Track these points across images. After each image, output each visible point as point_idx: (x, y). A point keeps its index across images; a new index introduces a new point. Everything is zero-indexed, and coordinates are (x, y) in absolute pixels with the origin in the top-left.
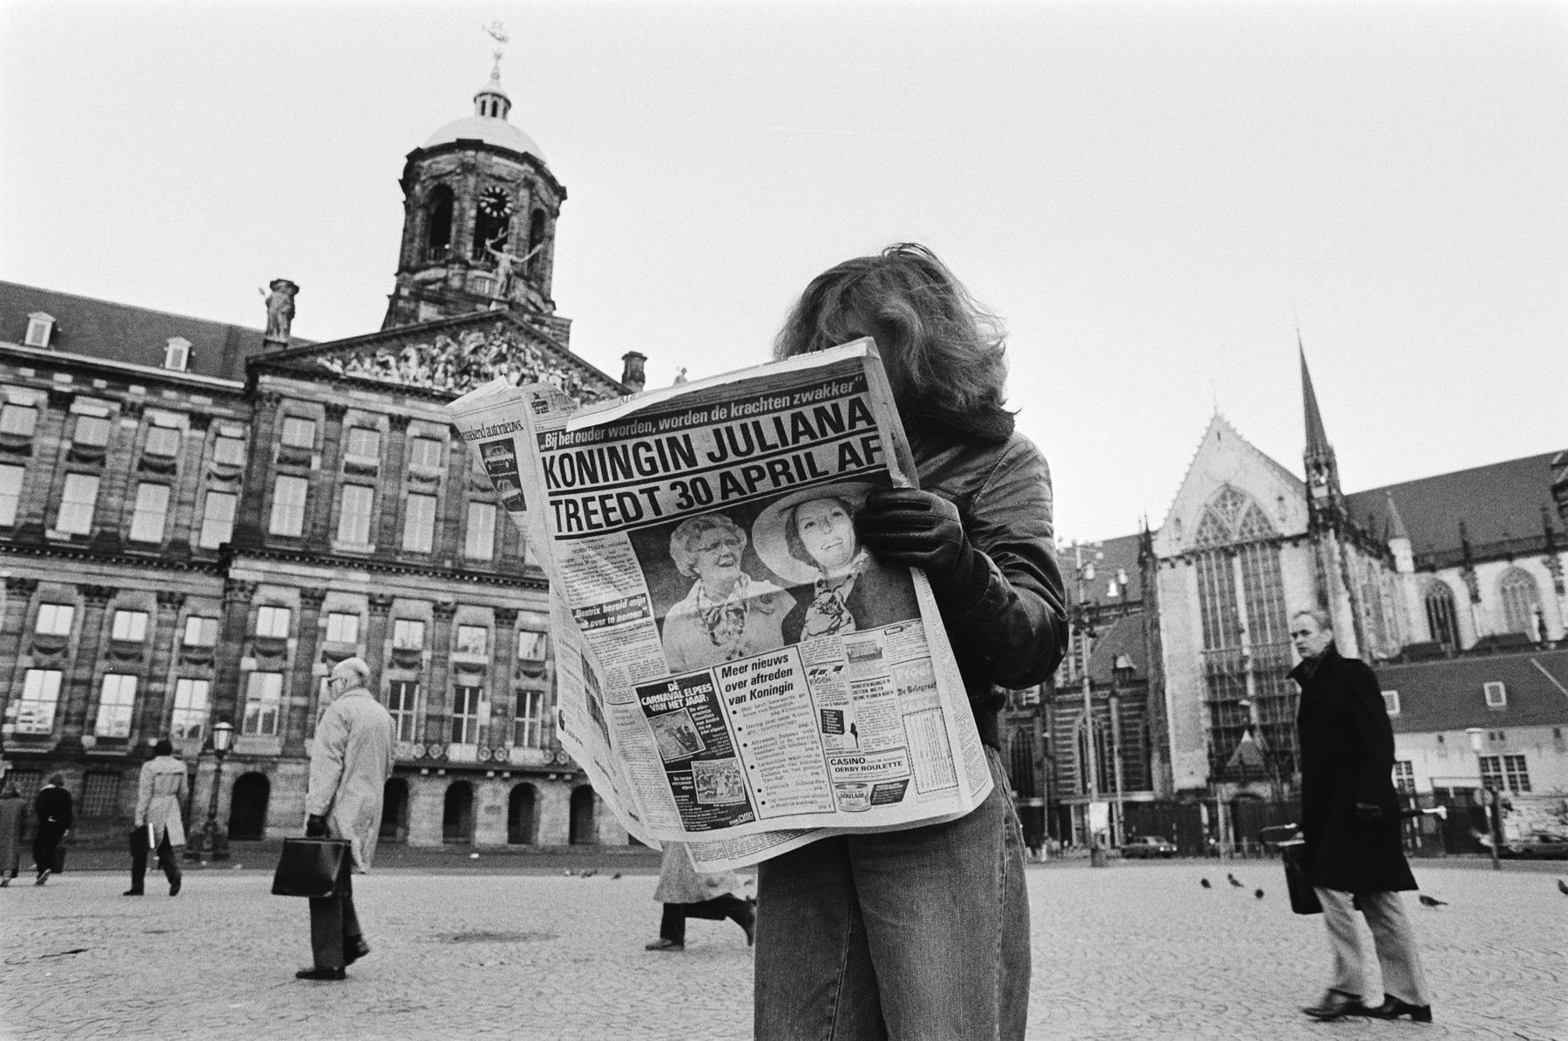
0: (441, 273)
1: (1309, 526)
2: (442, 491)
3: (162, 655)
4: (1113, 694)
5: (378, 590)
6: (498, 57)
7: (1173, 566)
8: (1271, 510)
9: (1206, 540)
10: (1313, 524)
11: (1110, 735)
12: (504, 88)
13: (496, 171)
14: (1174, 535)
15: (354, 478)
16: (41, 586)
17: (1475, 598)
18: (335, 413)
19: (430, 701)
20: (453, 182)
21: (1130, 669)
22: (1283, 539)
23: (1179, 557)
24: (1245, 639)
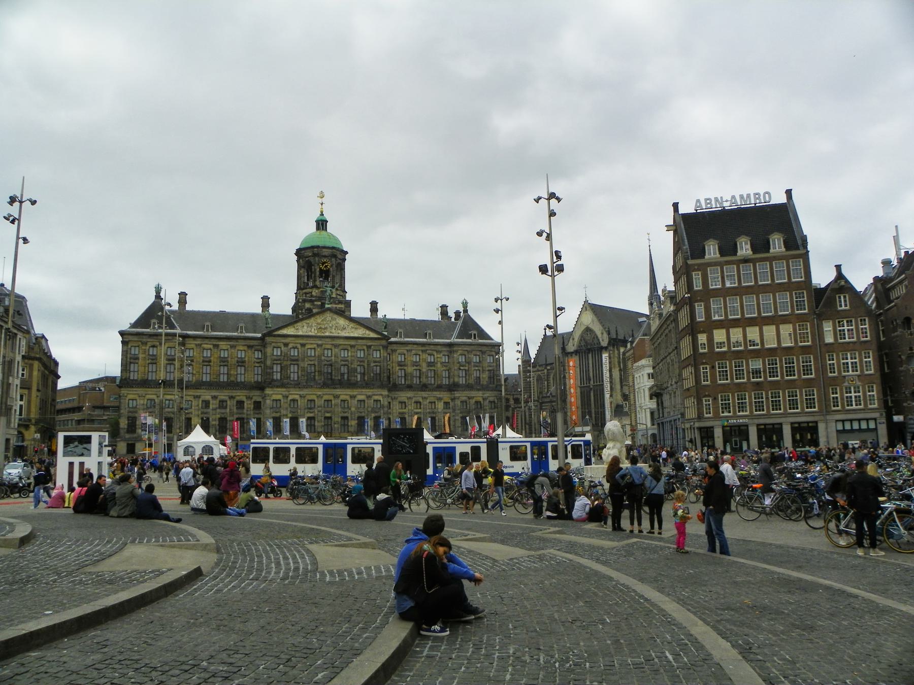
0: (310, 290)
2: (316, 363)
3: (249, 412)
5: (301, 393)
6: (322, 204)
8: (599, 336)
9: (582, 346)
10: (609, 343)
12: (327, 216)
13: (324, 254)
15: (293, 363)
16: (219, 397)
18: (286, 345)
19: (318, 422)
20: (312, 259)
23: (572, 353)
24: (592, 382)
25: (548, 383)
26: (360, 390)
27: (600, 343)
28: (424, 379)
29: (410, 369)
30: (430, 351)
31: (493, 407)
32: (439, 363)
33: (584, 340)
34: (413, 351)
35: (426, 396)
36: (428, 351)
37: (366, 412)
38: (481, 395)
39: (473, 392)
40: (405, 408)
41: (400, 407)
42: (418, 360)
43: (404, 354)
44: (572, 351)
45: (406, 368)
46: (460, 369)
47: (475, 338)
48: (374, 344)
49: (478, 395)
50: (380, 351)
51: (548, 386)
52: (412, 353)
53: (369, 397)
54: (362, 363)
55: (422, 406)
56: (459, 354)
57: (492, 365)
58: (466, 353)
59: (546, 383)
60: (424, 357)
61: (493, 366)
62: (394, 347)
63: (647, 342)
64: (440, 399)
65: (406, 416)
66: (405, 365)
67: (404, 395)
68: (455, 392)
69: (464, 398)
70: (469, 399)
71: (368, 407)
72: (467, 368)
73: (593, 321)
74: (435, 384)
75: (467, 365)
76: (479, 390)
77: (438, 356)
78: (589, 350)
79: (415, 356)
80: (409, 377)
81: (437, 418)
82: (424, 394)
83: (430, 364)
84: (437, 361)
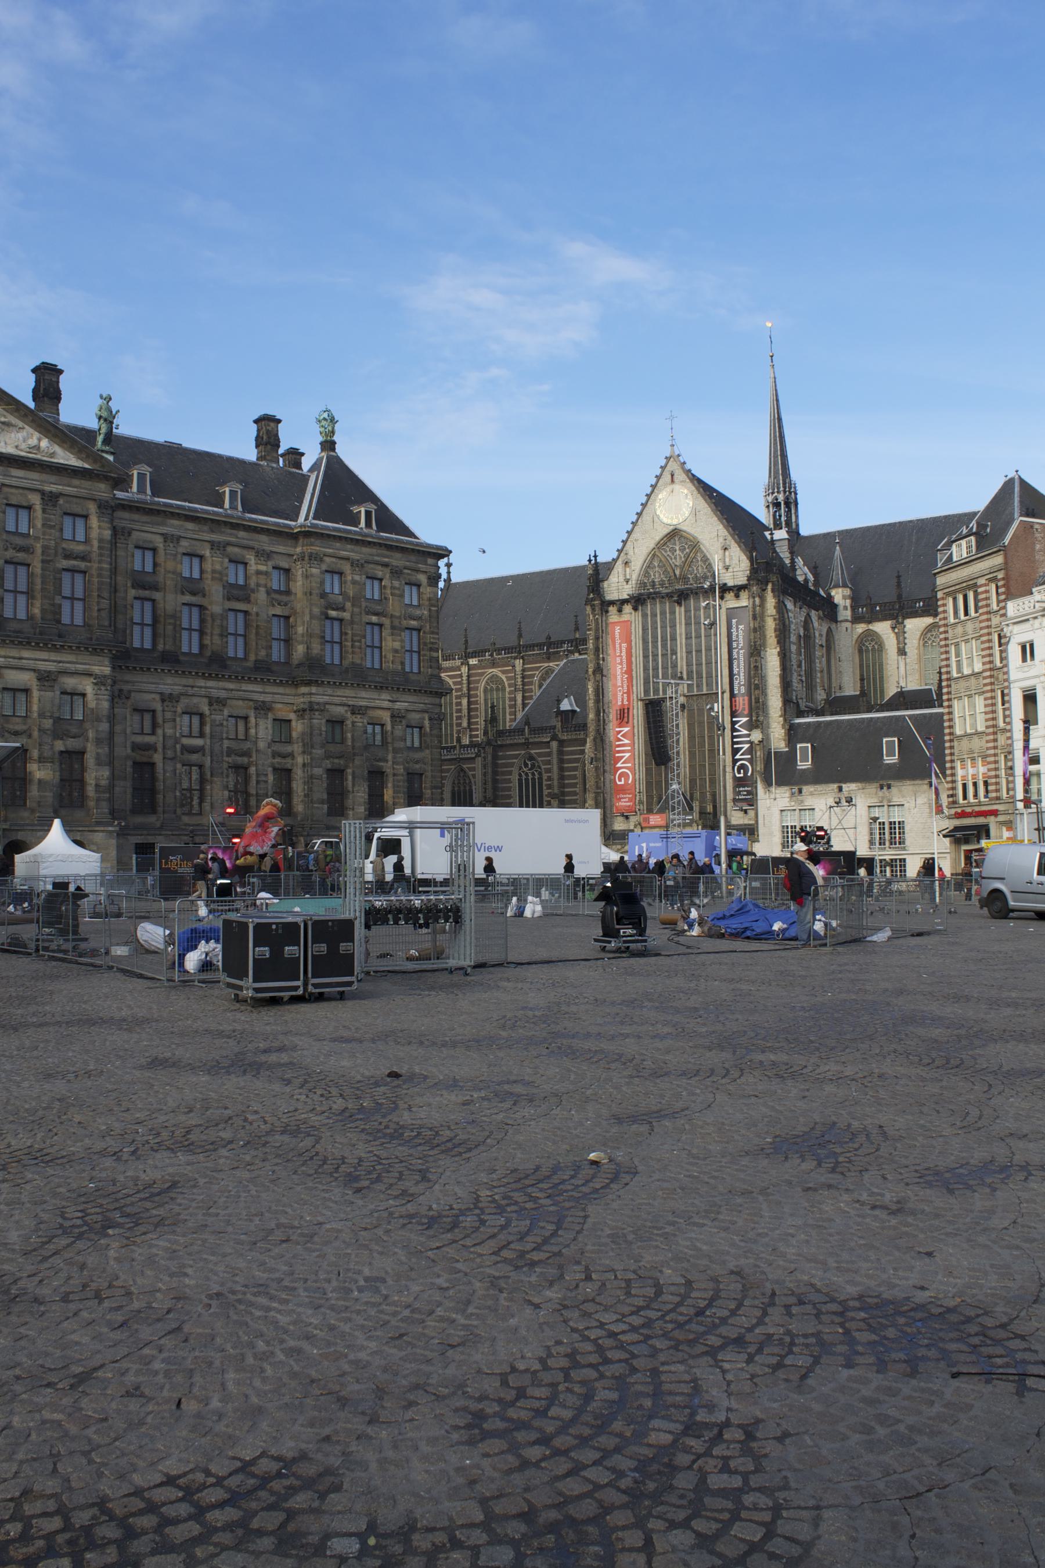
1: (749, 579)
4: (554, 738)
7: (620, 611)
11: (549, 779)
14: (622, 579)
17: (902, 652)
21: (574, 712)
23: (624, 602)
25: (469, 703)
26: (14, 653)
28: (217, 640)
29: (170, 601)
30: (236, 550)
31: (417, 744)
32: (262, 589)
33: (662, 566)
34: (184, 543)
35: (223, 694)
36: (230, 549)
37: (36, 734)
38: (386, 704)
39: (363, 694)
40: (153, 733)
41: (137, 727)
42: (196, 575)
43: (154, 550)
44: (626, 597)
45: (157, 596)
46: (327, 617)
47: (368, 524)
48: (68, 490)
49: (378, 703)
50: (86, 517)
51: (469, 710)
52: (181, 550)
53: (46, 679)
54: (21, 556)
55: (207, 729)
56: (324, 567)
57: (418, 612)
58: (346, 568)
59: (465, 701)
60: (218, 567)
61: (418, 618)
62: (124, 518)
63: (1037, 535)
64: (263, 708)
65: (158, 758)
66: (155, 587)
67: (152, 687)
68: (314, 690)
69: (341, 710)
70: (353, 713)
71: (42, 715)
72: (346, 615)
73: (695, 512)
74: (245, 659)
75: (348, 605)
76: (380, 687)
77: (263, 568)
78: (681, 597)
79: (186, 559)
80: (170, 628)
81: (252, 770)
82: (217, 688)
83: (239, 593)
84: (258, 585)
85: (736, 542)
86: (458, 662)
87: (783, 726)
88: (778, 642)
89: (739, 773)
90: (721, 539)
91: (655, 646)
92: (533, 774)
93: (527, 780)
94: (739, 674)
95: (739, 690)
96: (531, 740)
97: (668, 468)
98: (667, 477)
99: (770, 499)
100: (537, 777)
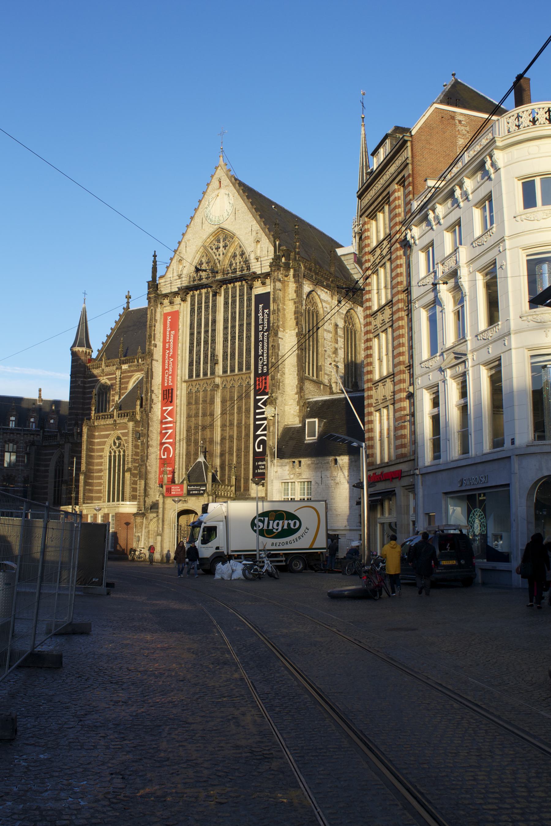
10: (275, 264)
14: (175, 274)
22: (255, 277)
23: (176, 294)
24: (219, 369)
27: (249, 268)
63: (460, 128)
85: (266, 235)
86: (115, 367)
87: (298, 403)
88: (297, 324)
89: (259, 448)
90: (254, 233)
91: (199, 333)
92: (120, 452)
93: (115, 456)
94: (263, 355)
95: (262, 370)
96: (118, 422)
97: (216, 176)
98: (215, 183)
99: (356, 229)
100: (122, 453)
